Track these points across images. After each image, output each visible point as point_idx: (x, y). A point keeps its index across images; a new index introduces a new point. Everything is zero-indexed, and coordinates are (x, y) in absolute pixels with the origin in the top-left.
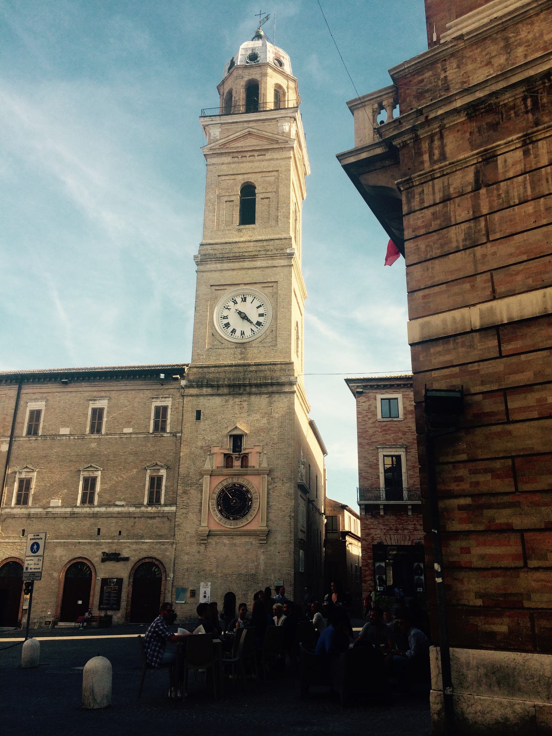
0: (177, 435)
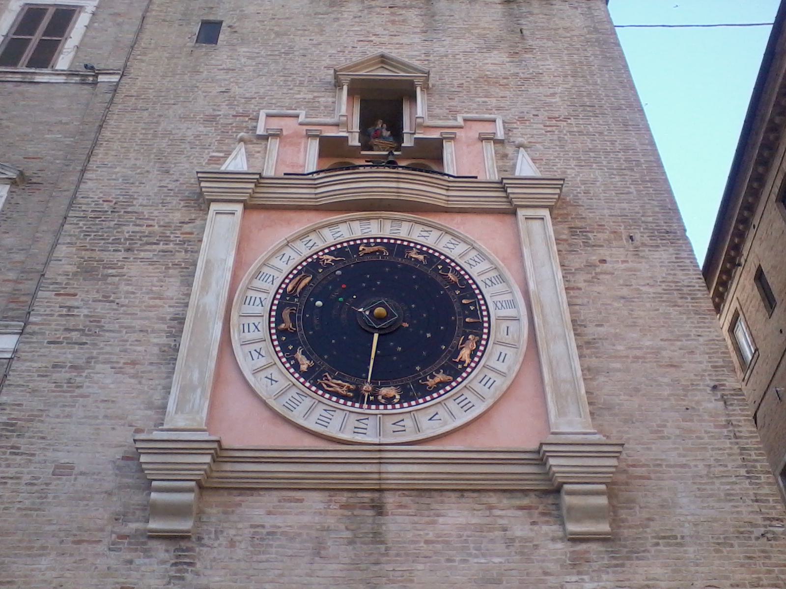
0: (101, 78)
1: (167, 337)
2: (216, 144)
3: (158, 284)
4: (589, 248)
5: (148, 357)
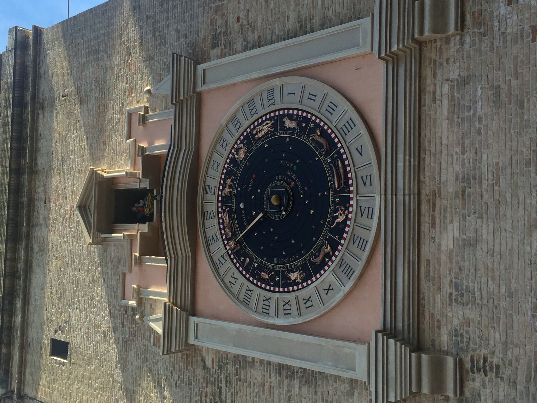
1: (294, 379)
2: (144, 341)
3: (252, 386)
4: (228, 32)
5: (310, 396)
